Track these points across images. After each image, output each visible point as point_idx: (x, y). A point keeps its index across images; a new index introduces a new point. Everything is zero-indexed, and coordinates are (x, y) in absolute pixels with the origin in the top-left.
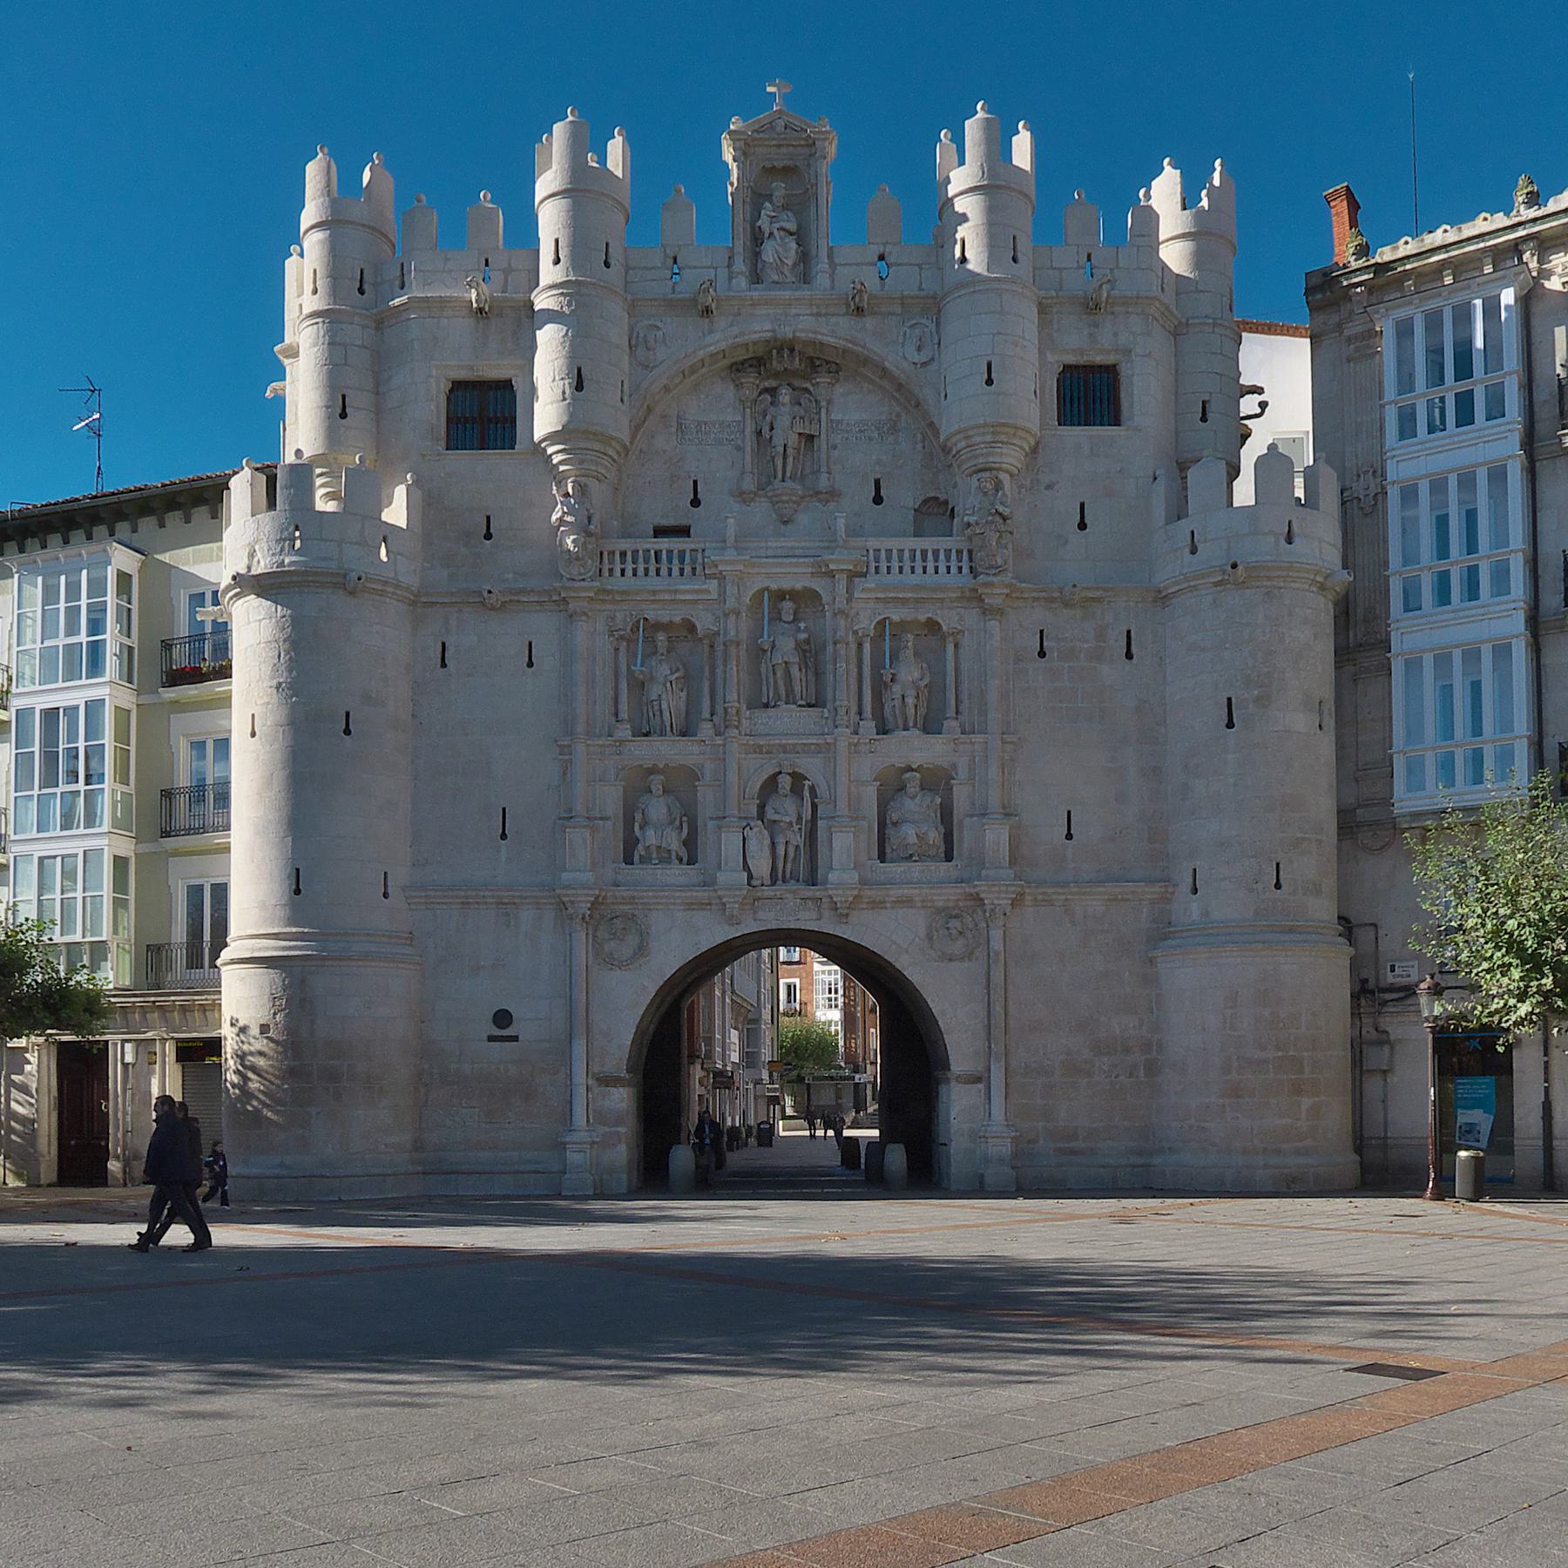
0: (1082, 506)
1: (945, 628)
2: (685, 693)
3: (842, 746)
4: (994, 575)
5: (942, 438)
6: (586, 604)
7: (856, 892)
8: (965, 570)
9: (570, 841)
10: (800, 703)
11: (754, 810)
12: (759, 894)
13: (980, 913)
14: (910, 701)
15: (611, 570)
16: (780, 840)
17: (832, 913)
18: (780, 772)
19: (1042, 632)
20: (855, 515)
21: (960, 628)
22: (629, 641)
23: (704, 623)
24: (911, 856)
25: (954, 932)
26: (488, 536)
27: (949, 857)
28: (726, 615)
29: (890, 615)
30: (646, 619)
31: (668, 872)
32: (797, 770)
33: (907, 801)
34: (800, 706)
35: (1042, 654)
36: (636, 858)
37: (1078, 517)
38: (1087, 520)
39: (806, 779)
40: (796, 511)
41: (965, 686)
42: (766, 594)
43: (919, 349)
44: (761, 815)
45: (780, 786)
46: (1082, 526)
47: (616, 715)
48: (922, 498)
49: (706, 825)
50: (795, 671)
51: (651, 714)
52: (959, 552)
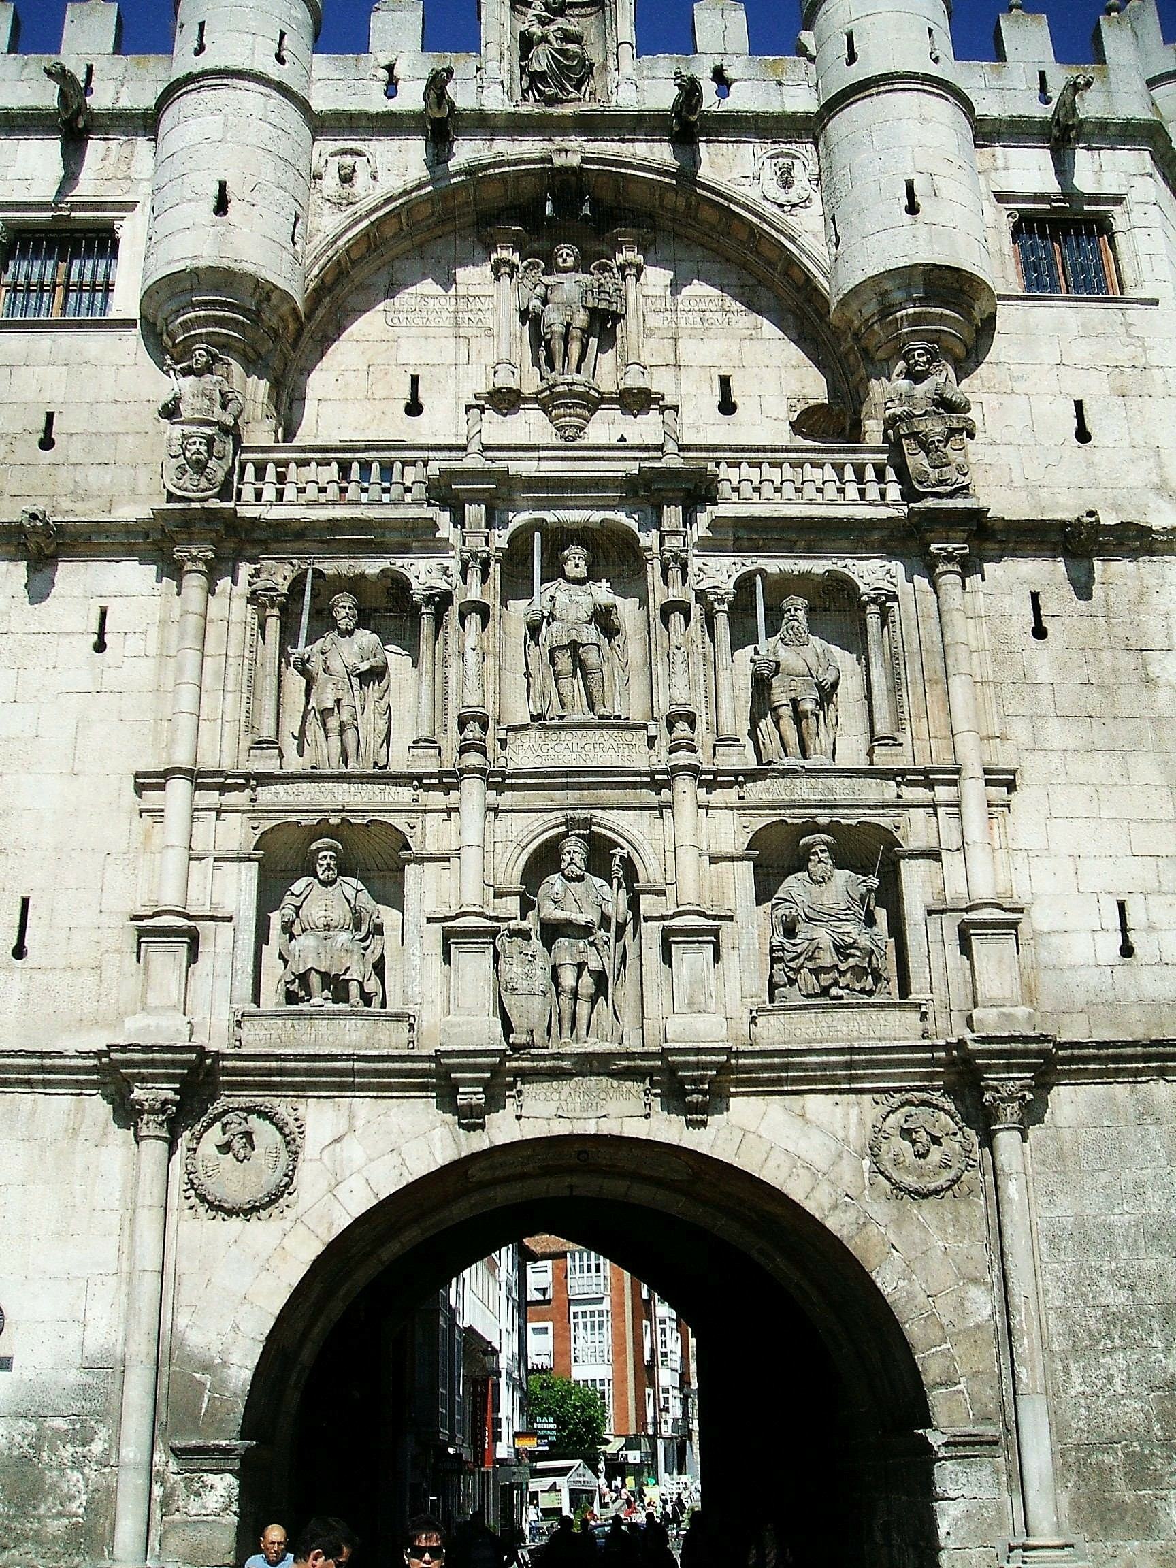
0: (1079, 405)
1: (863, 589)
4: (951, 495)
5: (833, 305)
8: (894, 491)
10: (602, 711)
11: (512, 905)
15: (258, 495)
18: (565, 835)
22: (284, 609)
24: (825, 991)
26: (47, 443)
30: (318, 574)
34: (602, 717)
37: (1074, 424)
38: (1089, 427)
42: (537, 535)
43: (787, 184)
44: (527, 906)
46: (1083, 435)
48: (801, 407)
50: (591, 657)
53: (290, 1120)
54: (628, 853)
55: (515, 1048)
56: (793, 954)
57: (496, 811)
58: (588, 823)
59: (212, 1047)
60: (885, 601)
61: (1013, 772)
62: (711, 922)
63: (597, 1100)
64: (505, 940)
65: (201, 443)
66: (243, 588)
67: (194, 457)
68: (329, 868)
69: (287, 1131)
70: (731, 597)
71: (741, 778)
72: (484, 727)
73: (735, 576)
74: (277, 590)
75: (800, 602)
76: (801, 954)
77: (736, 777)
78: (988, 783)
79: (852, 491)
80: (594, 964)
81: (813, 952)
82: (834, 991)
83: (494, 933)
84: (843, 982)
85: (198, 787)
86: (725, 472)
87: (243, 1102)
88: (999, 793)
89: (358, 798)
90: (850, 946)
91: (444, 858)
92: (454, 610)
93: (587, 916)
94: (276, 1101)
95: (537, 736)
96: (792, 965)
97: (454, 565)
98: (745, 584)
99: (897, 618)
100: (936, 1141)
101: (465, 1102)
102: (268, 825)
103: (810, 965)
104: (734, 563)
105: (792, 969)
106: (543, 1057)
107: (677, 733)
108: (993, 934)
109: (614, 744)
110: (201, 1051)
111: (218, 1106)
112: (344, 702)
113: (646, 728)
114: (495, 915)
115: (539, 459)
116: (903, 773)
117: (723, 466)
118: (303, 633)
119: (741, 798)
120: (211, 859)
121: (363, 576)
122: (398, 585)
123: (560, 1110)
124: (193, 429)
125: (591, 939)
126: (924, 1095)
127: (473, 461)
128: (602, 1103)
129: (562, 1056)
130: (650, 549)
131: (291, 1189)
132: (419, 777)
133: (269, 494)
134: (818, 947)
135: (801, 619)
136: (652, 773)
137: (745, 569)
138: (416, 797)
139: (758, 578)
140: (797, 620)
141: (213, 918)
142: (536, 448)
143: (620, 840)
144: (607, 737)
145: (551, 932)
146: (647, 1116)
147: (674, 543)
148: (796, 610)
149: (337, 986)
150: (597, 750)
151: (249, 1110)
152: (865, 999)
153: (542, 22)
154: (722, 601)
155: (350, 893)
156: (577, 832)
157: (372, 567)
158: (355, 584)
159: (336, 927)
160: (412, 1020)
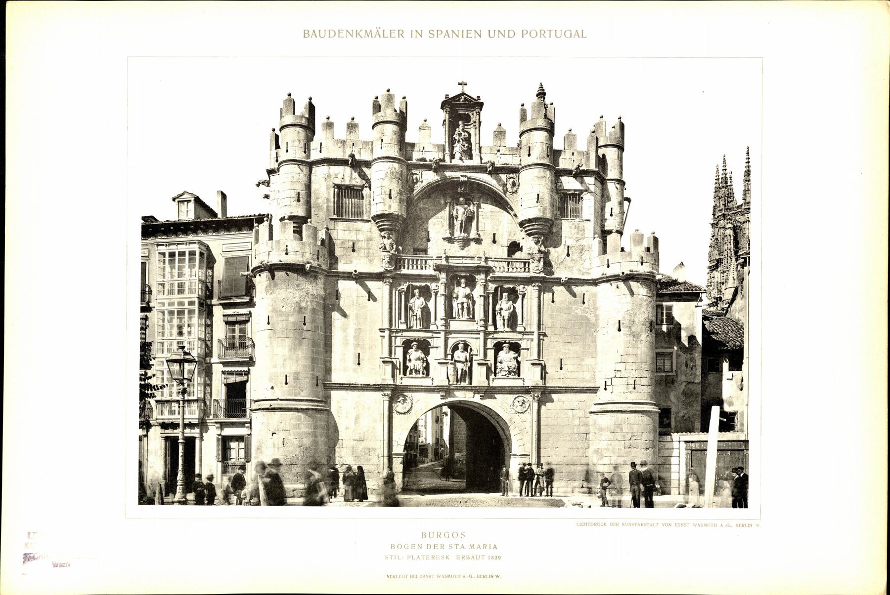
4: (539, 273)
11: (449, 357)
14: (506, 318)
18: (460, 343)
22: (405, 293)
23: (433, 286)
24: (506, 375)
30: (412, 285)
39: (469, 346)
47: (401, 319)
50: (465, 305)
55: (450, 385)
58: (465, 341)
82: (507, 375)
83: (447, 363)
93: (463, 360)
98: (496, 289)
102: (404, 340)
118: (410, 296)
121: (421, 286)
122: (427, 288)
132: (433, 331)
141: (395, 358)
145: (456, 361)
149: (417, 371)
153: (460, 135)
157: (423, 284)
158: (419, 288)
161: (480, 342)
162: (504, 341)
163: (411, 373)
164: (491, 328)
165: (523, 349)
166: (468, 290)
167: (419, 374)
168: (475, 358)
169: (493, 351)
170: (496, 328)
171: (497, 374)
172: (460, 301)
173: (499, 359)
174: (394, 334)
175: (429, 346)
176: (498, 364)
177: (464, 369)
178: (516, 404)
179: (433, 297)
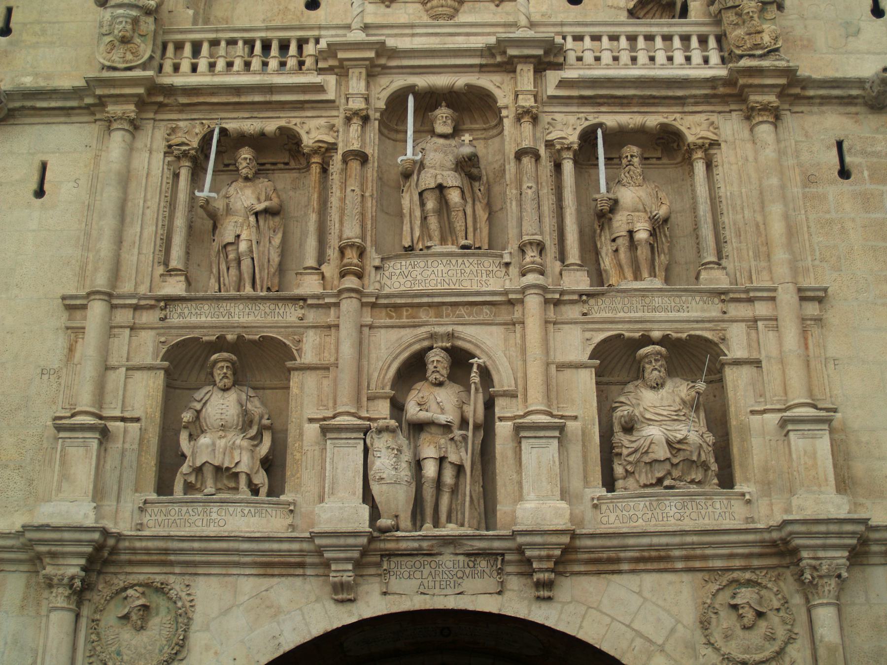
1: (691, 139)
2: (280, 235)
3: (533, 302)
6: (132, 107)
7: (566, 539)
8: (714, 58)
9: (63, 456)
10: (463, 242)
11: (383, 409)
12: (391, 545)
13: (790, 579)
14: (642, 235)
16: (429, 451)
17: (523, 580)
18: (431, 348)
19: (840, 145)
20: (542, 15)
21: (715, 137)
22: (194, 160)
24: (660, 481)
25: (750, 615)
27: (727, 481)
28: (348, 120)
29: (604, 121)
30: (223, 132)
31: (231, 509)
32: (460, 343)
33: (648, 397)
34: (464, 247)
35: (844, 173)
36: (178, 486)
39: (473, 356)
40: (457, 11)
41: (727, 219)
42: (411, 100)
45: (431, 367)
47: (166, 263)
49: (301, 434)
50: (454, 196)
51: (223, 267)
52: (703, 40)
53: (183, 595)
54: (484, 363)
55: (384, 531)
56: (630, 450)
57: (371, 327)
58: (451, 336)
59: (113, 528)
60: (710, 146)
61: (825, 290)
62: (557, 420)
63: (455, 576)
64: (375, 436)
65: (126, 22)
66: (160, 144)
67: (120, 34)
68: (225, 376)
69: (179, 604)
70: (576, 146)
71: (584, 298)
72: (362, 253)
73: (579, 129)
74: (187, 145)
75: (635, 150)
76: (636, 451)
77: (581, 295)
78: (803, 299)
79: (679, 57)
80: (453, 457)
81: (649, 447)
83: (366, 431)
84: (676, 473)
85: (113, 307)
86: (570, 43)
87: (142, 578)
88: (812, 309)
89: (251, 318)
90: (680, 442)
91: (326, 368)
92: (338, 157)
93: (449, 416)
94: (172, 579)
95: (408, 262)
96: (631, 459)
97: (339, 122)
98: (588, 137)
99: (719, 161)
100: (760, 615)
101: (336, 579)
103: (647, 459)
104: (578, 118)
105: (630, 463)
106: (404, 538)
107: (528, 259)
108: (809, 430)
109: (474, 270)
110: (105, 532)
111: (119, 582)
112: (243, 237)
113: (501, 256)
114: (368, 415)
115: (413, 35)
116: (726, 292)
117: (569, 39)
119: (584, 314)
120: (124, 369)
121: (262, 134)
123: (422, 587)
124: (120, 11)
125: (451, 436)
126: (748, 575)
127: (358, 36)
128: (460, 581)
129: (425, 538)
130: (506, 107)
131: (180, 657)
133: (185, 66)
134: (651, 443)
135: (636, 164)
136: (506, 293)
137: (587, 124)
138: (301, 315)
139: (599, 132)
140: (633, 165)
141: (123, 419)
142: (412, 26)
143: (477, 352)
144: (467, 264)
145: (418, 428)
146: (500, 593)
147: (527, 102)
148: (632, 156)
150: (459, 275)
151: (147, 585)
152: (694, 488)
154: (569, 149)
155: (244, 397)
156: (440, 344)
157: (271, 126)
159: (230, 428)
160: (292, 508)
161: (523, 337)
162: (637, 335)
163: (189, 487)
164: (579, 281)
165: (737, 363)
166: (467, 142)
167: (236, 489)
168: (502, 407)
169: (586, 381)
170: (599, 277)
171: (620, 484)
172: (428, 180)
173: (621, 412)
174: (124, 317)
175: (289, 364)
176: (620, 437)
177: (453, 457)
178: (726, 620)
179: (315, 169)
